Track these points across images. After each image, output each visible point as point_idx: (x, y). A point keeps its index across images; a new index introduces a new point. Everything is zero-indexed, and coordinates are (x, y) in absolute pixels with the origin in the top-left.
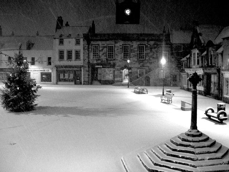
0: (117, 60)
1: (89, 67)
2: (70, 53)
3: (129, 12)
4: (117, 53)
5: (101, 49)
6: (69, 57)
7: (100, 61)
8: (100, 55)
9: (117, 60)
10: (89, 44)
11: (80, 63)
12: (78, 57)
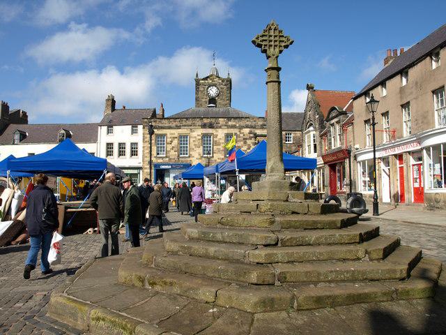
0: (193, 157)
2: (122, 146)
3: (211, 92)
4: (194, 147)
5: (169, 140)
6: (121, 153)
7: (167, 159)
9: (193, 157)
10: (151, 133)
11: (136, 161)
12: (134, 153)
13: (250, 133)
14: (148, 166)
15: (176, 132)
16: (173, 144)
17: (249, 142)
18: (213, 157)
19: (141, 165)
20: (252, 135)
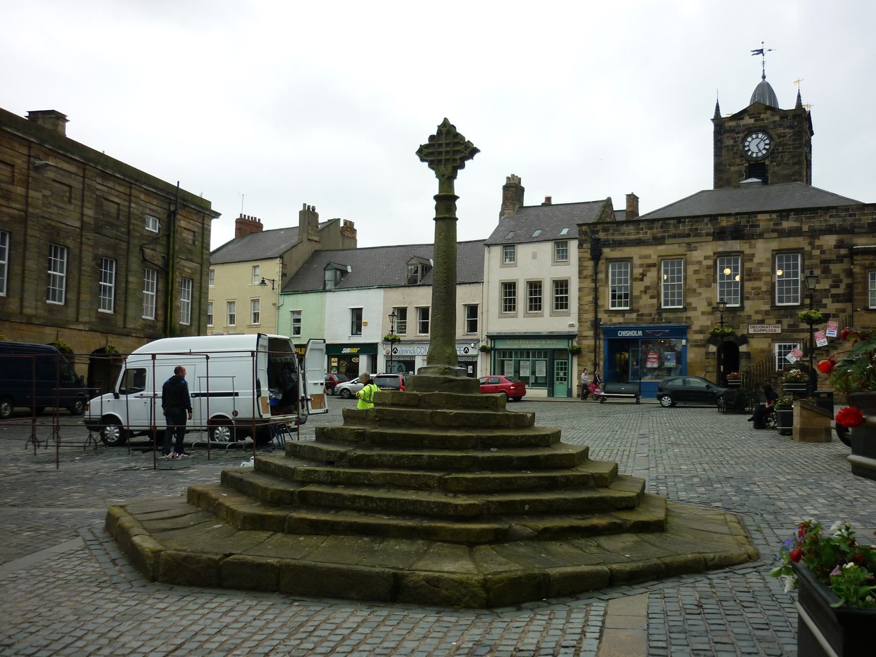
0: (695, 309)
1: (596, 337)
2: (535, 287)
3: (753, 148)
4: (695, 286)
5: (638, 271)
6: (535, 304)
7: (634, 316)
8: (636, 293)
9: (695, 309)
10: (596, 256)
11: (566, 322)
12: (561, 303)
13: (840, 245)
14: (591, 333)
15: (653, 252)
16: (647, 281)
17: (836, 268)
18: (742, 308)
19: (575, 330)
20: (843, 251)
